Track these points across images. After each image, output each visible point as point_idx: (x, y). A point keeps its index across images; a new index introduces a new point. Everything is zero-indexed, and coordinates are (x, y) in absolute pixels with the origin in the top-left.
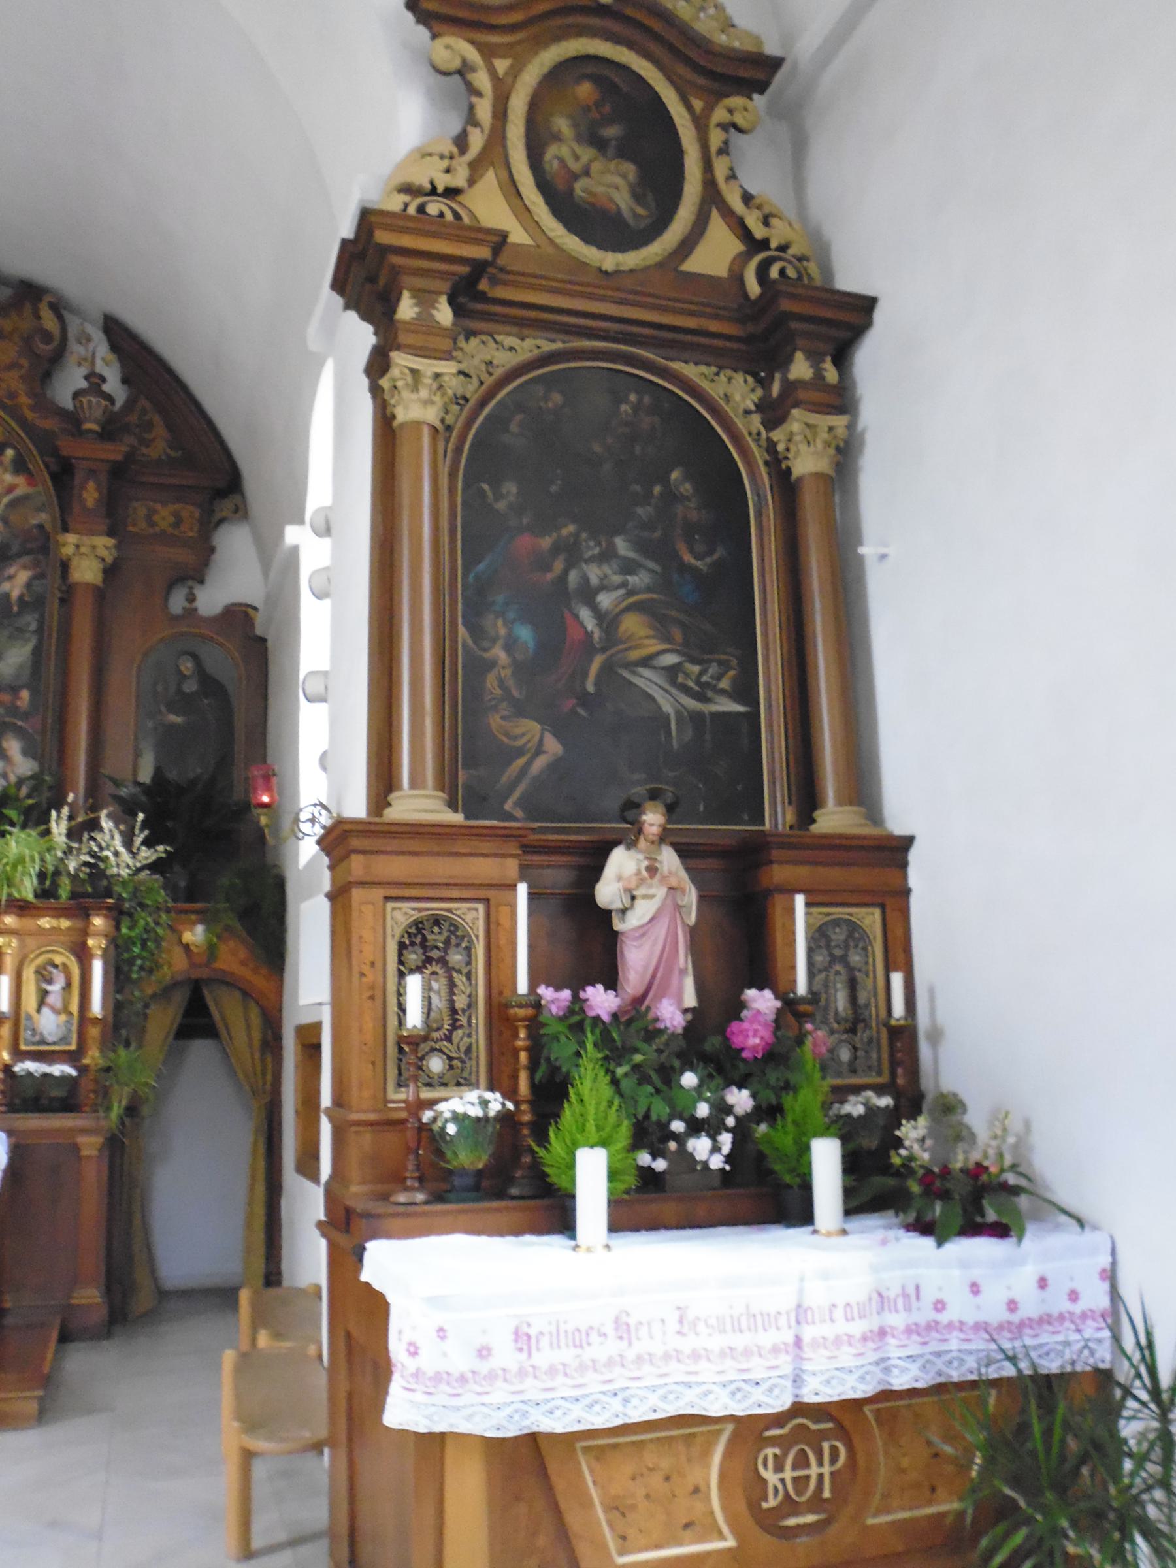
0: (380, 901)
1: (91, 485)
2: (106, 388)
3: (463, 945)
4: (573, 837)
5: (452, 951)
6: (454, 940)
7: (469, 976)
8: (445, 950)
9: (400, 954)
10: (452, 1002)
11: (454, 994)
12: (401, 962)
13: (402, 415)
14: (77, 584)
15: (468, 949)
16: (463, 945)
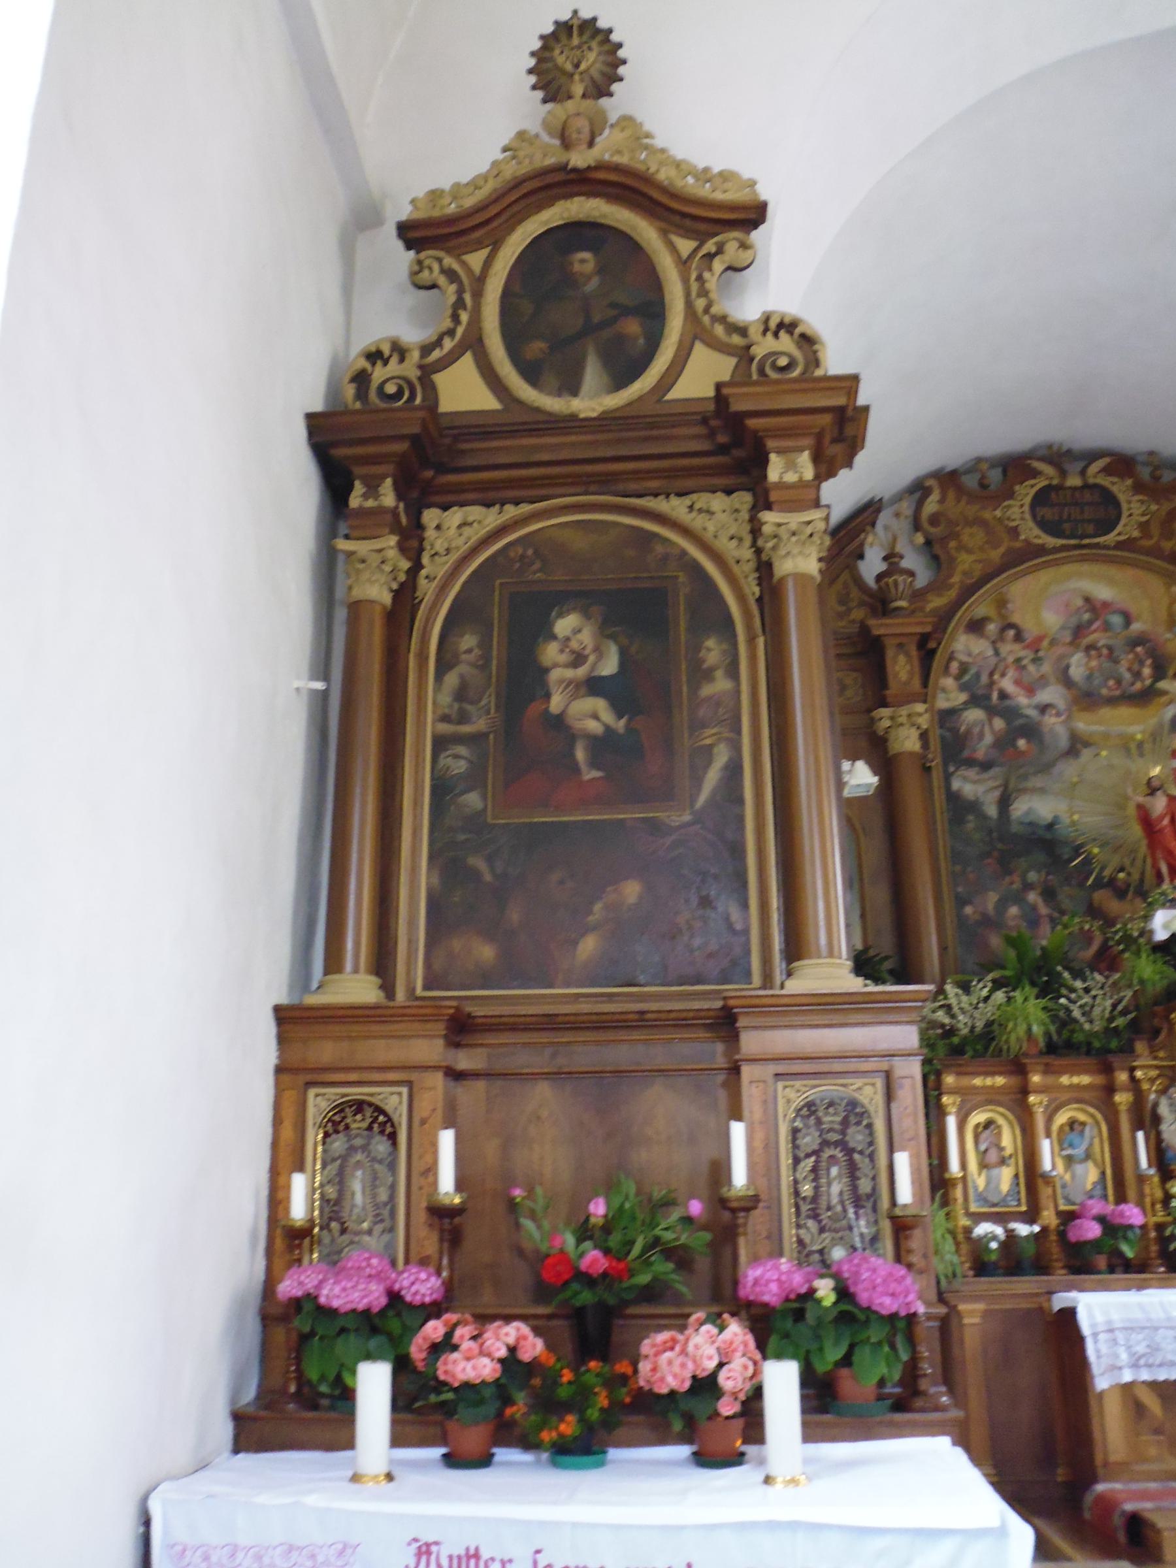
0: (770, 1080)
1: (902, 659)
2: (905, 564)
3: (865, 1123)
4: (697, 1005)
5: (851, 1131)
6: (853, 1119)
7: (872, 1157)
8: (843, 1133)
9: (794, 1139)
10: (854, 1188)
11: (858, 1179)
12: (795, 1147)
13: (785, 567)
14: (900, 754)
15: (870, 1126)
16: (865, 1123)
